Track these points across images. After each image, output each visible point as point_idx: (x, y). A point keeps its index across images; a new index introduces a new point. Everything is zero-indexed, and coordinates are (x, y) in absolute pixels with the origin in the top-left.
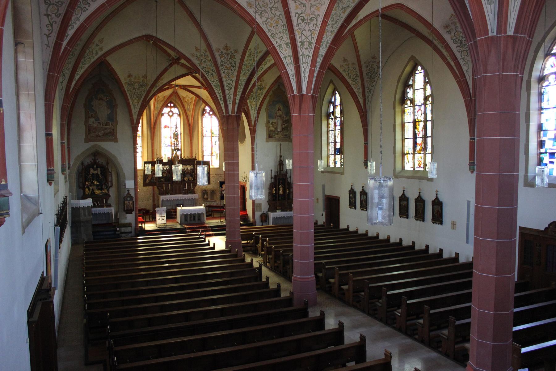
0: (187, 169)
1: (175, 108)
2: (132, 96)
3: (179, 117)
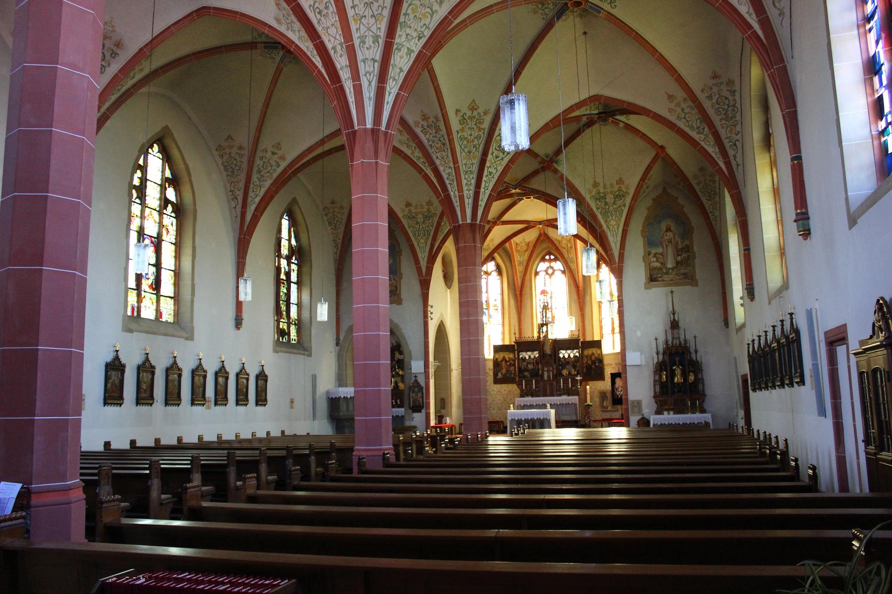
0: (569, 356)
2: (415, 234)
3: (563, 276)
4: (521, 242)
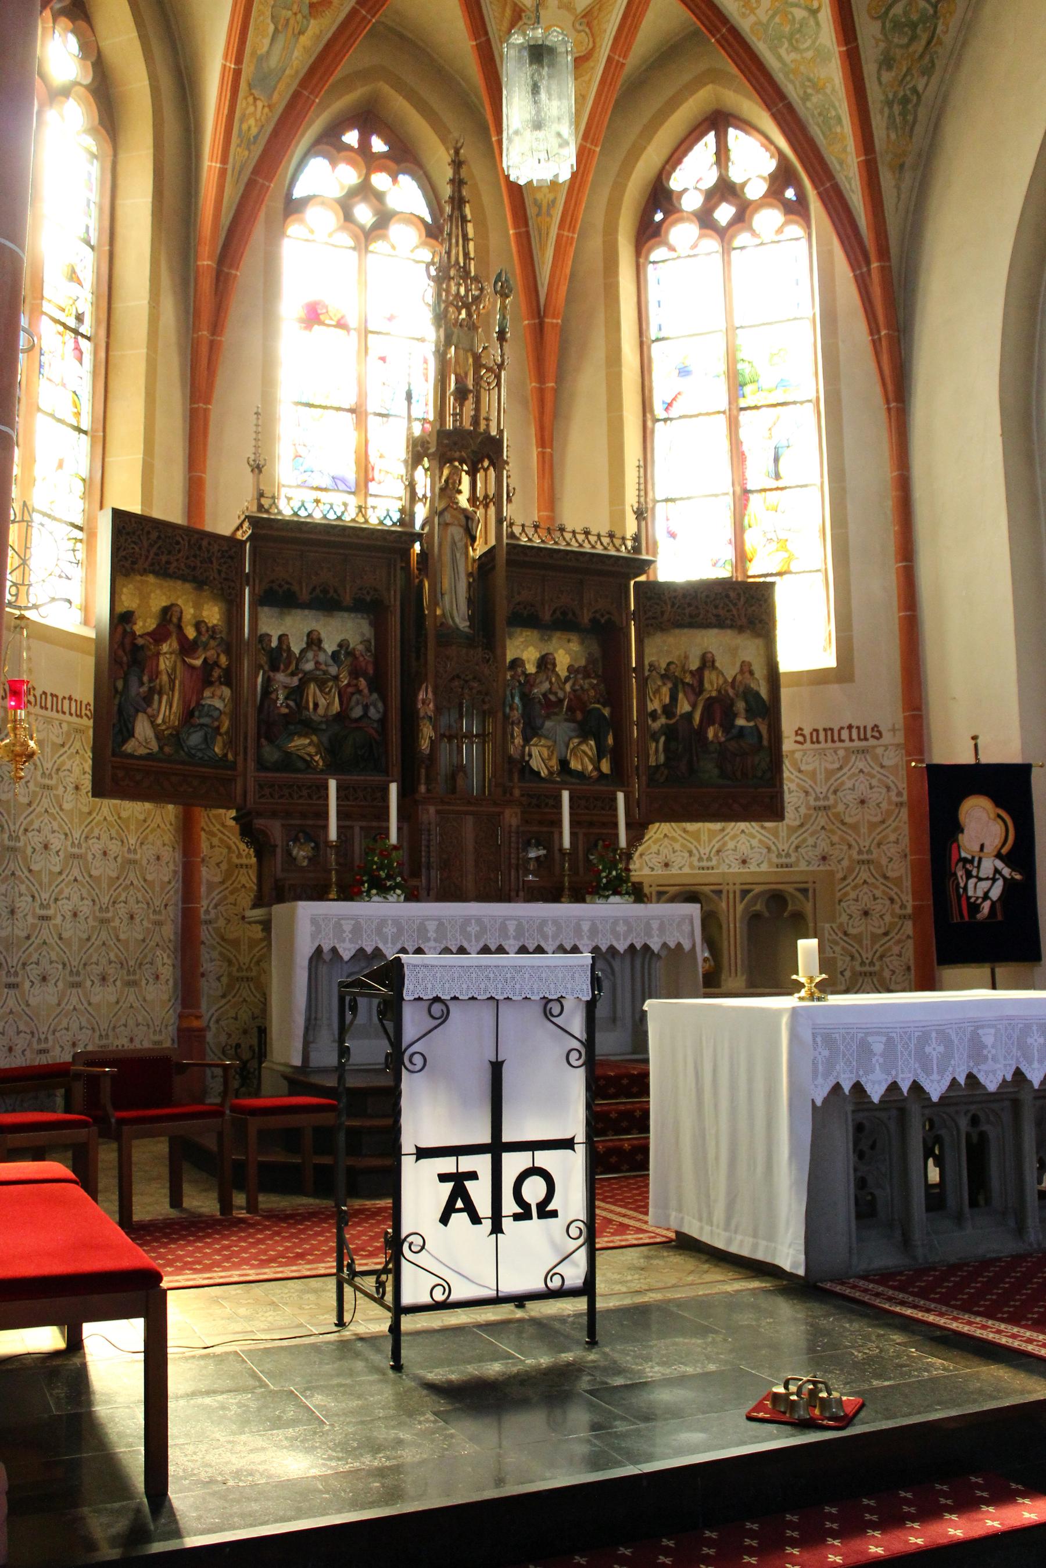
1: (405, 179)
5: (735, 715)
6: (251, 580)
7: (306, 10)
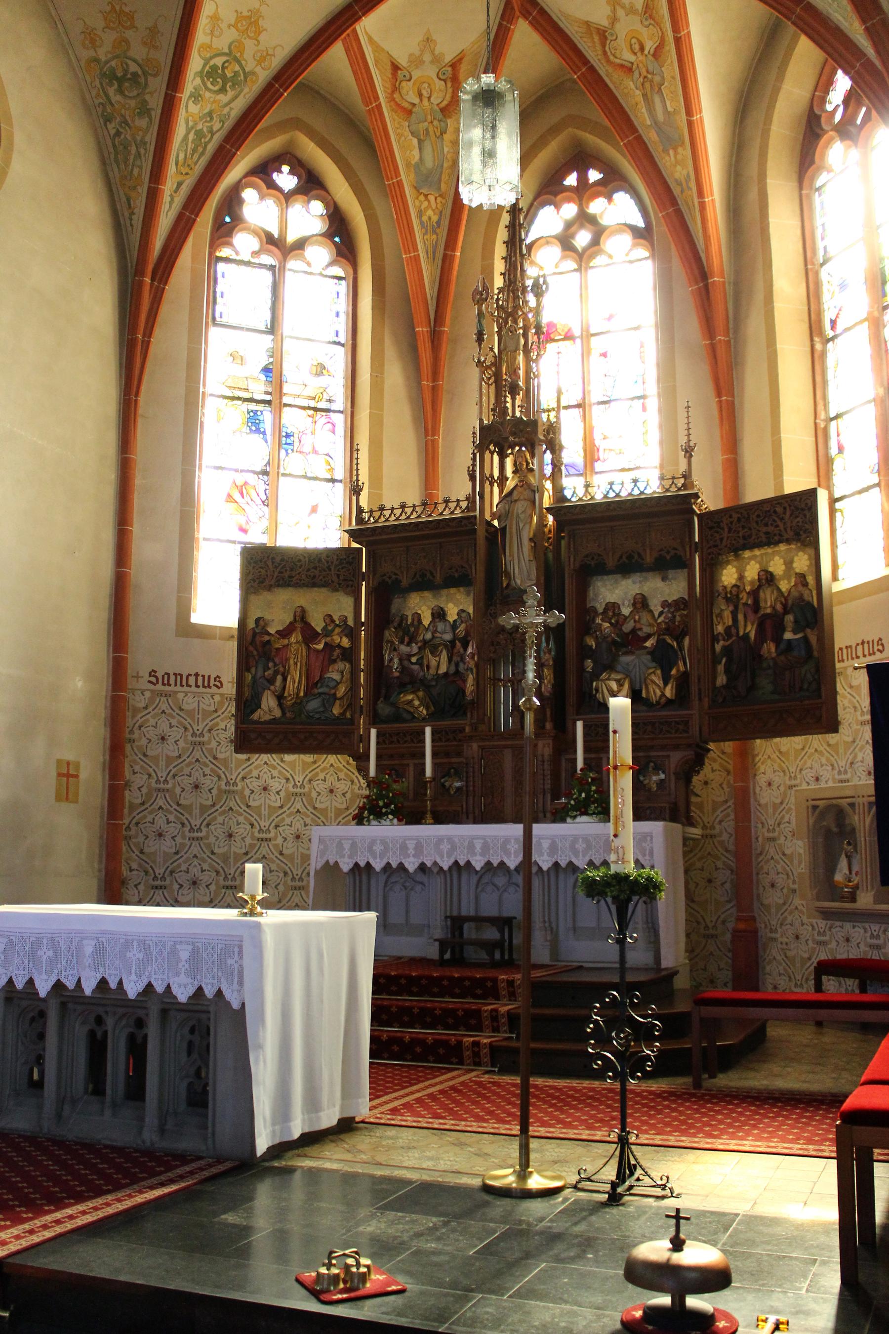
4: (417, 61)
5: (783, 630)
6: (366, 577)
7: (439, 116)
